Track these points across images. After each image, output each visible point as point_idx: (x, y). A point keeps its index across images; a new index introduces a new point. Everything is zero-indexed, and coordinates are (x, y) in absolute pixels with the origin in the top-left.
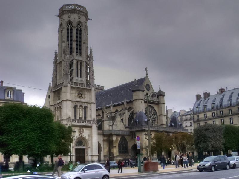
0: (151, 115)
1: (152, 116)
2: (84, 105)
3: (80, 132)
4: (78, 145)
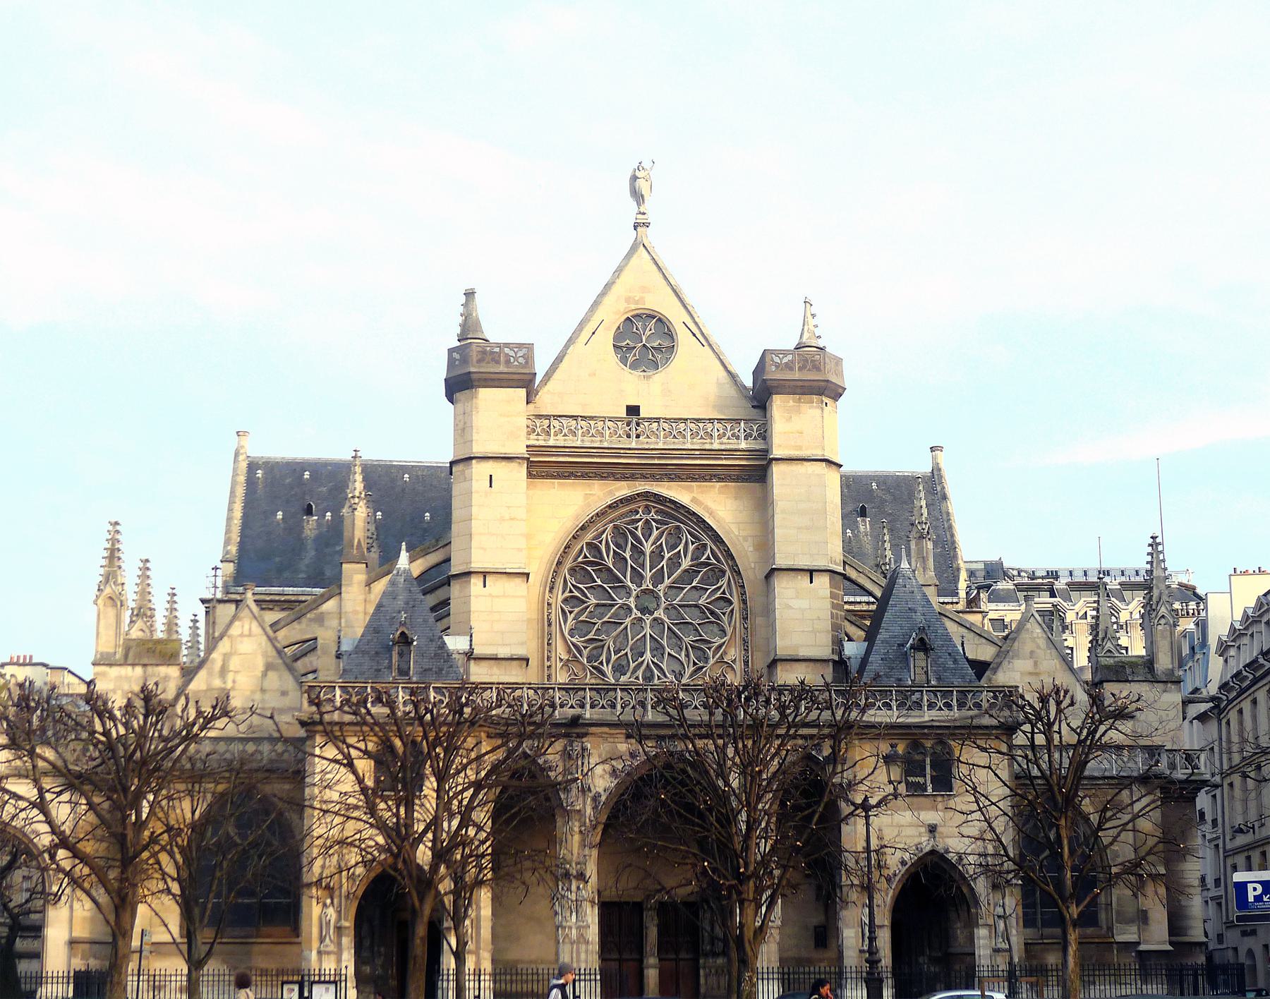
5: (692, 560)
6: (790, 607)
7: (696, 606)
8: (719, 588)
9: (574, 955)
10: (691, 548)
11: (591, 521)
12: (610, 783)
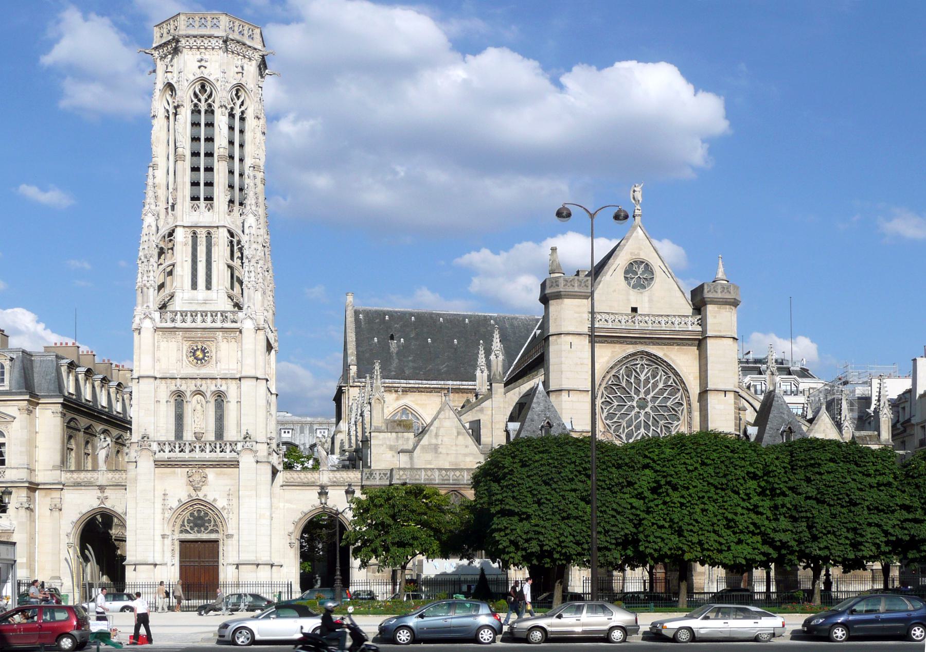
0: (649, 397)
1: (655, 398)
2: (210, 387)
3: (192, 486)
4: (192, 529)
5: (664, 384)
6: (715, 408)
7: (666, 406)
8: (677, 398)
11: (615, 365)
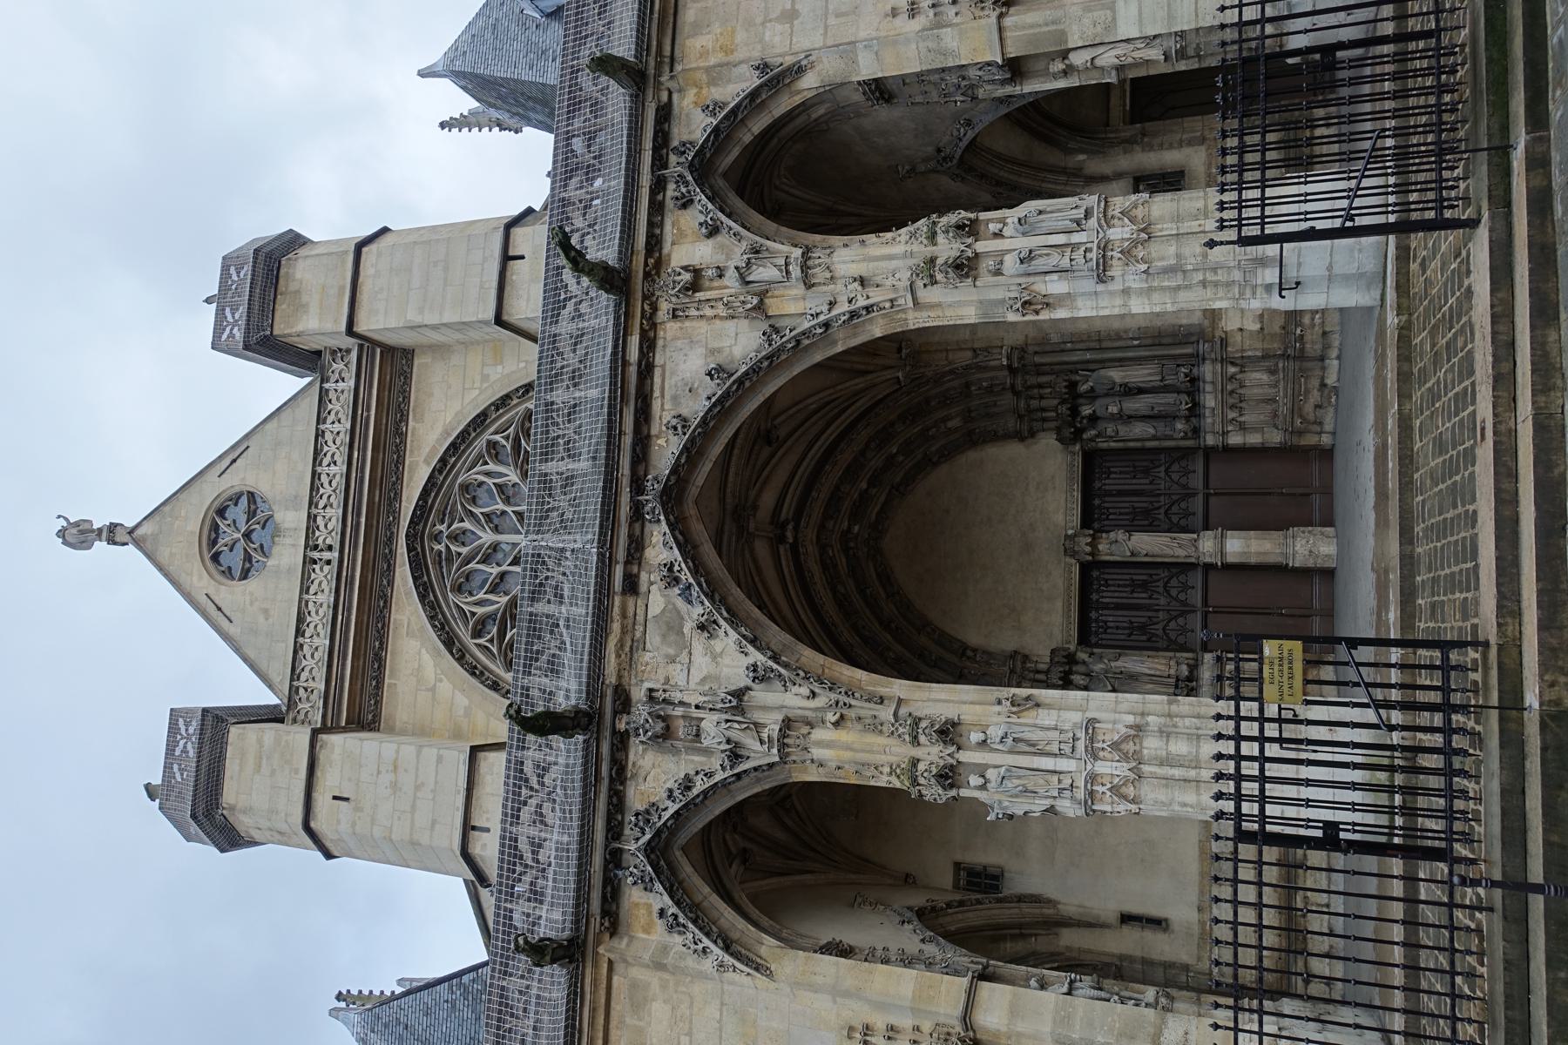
9: (1177, 772)
10: (491, 467)
12: (727, 639)
